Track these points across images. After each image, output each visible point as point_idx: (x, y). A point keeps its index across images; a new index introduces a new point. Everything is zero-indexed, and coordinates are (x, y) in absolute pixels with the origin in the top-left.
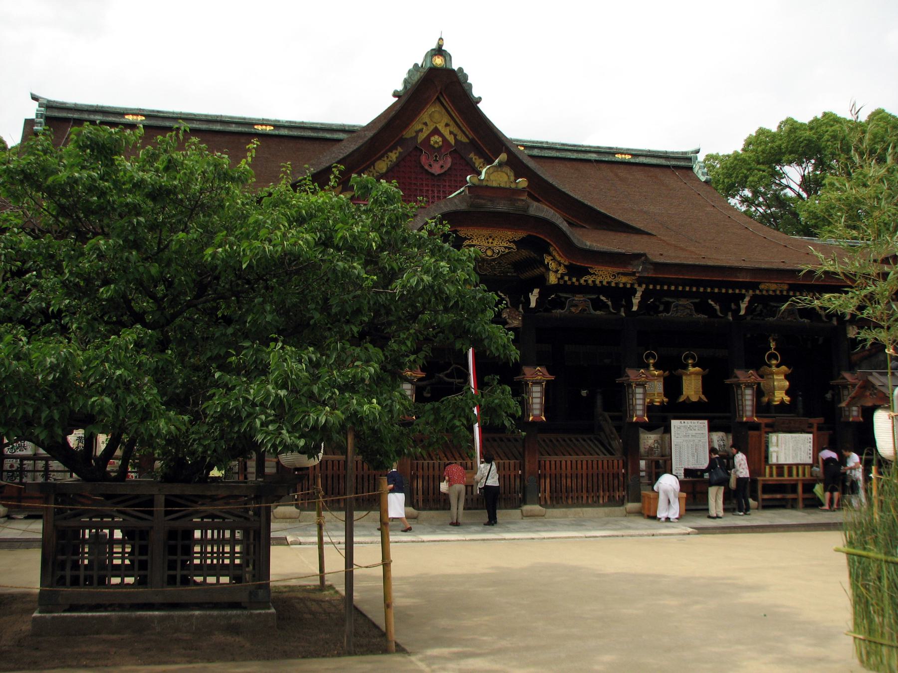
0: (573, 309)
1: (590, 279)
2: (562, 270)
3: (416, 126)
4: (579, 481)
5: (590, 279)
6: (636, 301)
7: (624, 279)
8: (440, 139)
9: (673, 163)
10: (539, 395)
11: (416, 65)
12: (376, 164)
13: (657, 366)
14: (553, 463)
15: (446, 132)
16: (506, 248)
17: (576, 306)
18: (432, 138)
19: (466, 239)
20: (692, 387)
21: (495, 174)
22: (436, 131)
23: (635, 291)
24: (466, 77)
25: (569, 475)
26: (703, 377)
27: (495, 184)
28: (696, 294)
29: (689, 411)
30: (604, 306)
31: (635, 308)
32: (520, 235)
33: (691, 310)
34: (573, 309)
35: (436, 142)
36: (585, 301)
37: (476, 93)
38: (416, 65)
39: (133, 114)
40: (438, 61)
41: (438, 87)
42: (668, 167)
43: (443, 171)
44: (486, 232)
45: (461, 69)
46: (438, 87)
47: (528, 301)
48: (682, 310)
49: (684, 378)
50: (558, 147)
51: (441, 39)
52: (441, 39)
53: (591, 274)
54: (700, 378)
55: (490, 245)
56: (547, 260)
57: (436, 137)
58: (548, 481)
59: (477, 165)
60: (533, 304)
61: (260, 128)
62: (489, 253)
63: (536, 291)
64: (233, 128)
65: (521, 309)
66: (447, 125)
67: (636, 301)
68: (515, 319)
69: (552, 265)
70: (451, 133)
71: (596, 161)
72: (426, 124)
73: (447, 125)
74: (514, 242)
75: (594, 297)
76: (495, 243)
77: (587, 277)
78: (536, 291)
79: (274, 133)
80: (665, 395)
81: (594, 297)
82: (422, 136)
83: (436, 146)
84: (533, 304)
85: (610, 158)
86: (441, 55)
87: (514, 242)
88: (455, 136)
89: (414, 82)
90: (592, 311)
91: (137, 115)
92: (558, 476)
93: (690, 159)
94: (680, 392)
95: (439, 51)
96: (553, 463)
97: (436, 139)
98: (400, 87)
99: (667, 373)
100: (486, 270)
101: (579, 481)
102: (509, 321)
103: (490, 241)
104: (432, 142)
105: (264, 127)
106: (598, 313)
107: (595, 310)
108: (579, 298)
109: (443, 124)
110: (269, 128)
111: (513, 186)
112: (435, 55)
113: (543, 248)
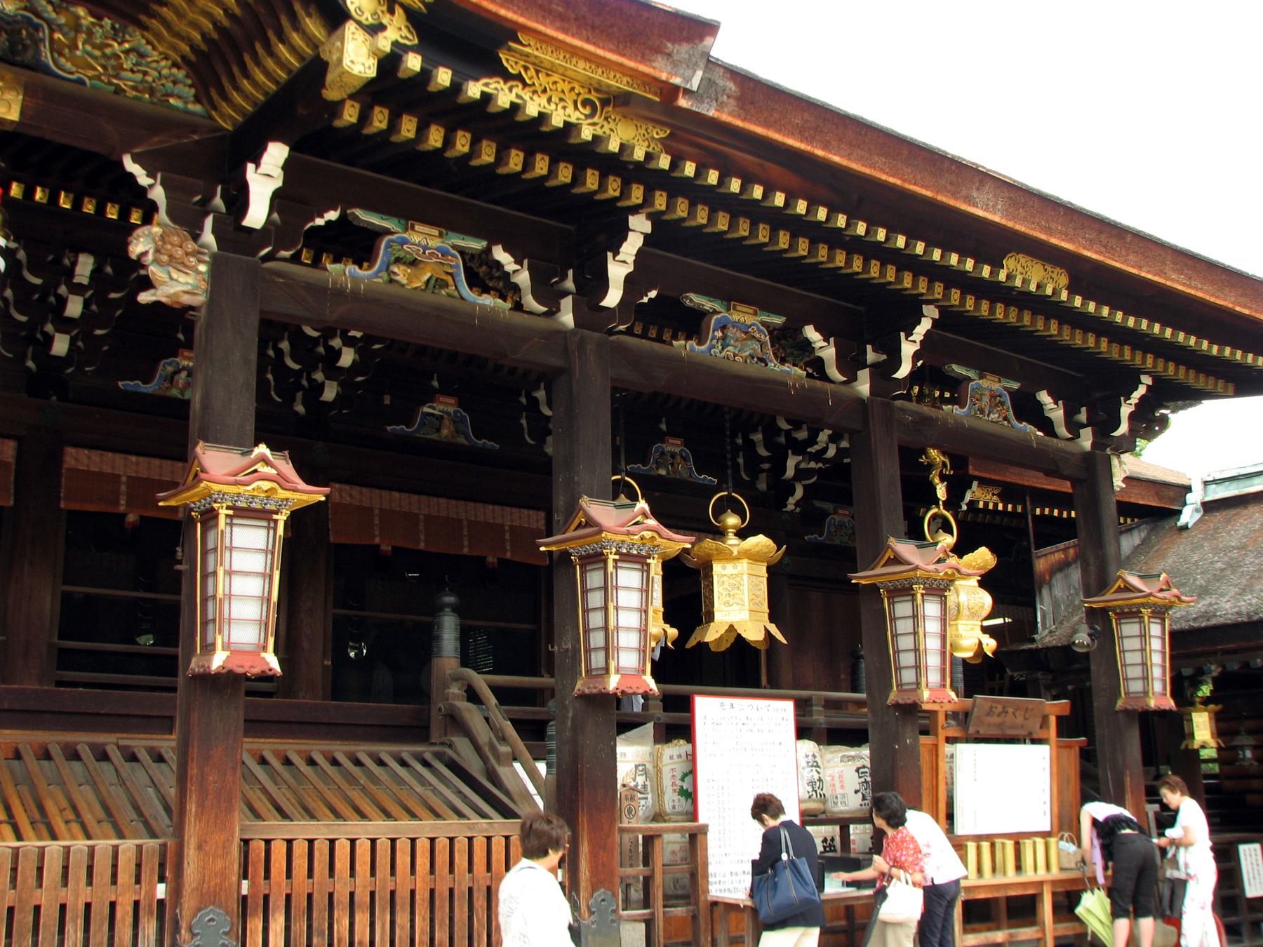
4: (402, 919)
6: (618, 270)
10: (257, 563)
14: (300, 849)
20: (740, 601)
23: (622, 233)
25: (362, 898)
26: (769, 569)
29: (740, 669)
30: (507, 288)
31: (613, 298)
33: (762, 345)
49: (717, 568)
53: (507, 76)
54: (762, 570)
58: (277, 924)
63: (276, 154)
65: (208, 237)
67: (618, 270)
68: (181, 266)
75: (477, 245)
78: (276, 154)
81: (477, 245)
92: (320, 903)
96: (300, 849)
101: (402, 919)
102: (155, 271)
106: (488, 300)
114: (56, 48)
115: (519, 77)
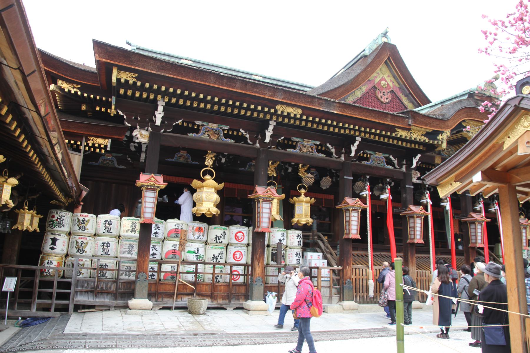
3: (375, 74)
15: (388, 80)
18: (382, 82)
22: (383, 79)
41: (387, 55)
70: (391, 81)
82: (377, 80)
83: (384, 87)
104: (382, 84)
109: (387, 76)
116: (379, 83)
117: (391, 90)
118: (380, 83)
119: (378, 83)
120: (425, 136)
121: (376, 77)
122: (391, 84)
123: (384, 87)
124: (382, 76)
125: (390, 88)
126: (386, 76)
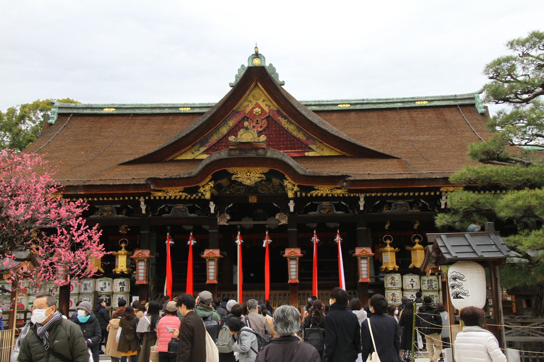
0: (322, 211)
1: (314, 193)
2: (296, 189)
5: (314, 193)
7: (339, 191)
8: (260, 110)
9: (460, 102)
11: (243, 66)
12: (220, 130)
13: (391, 245)
16: (259, 177)
17: (324, 209)
18: (255, 110)
19: (233, 174)
21: (245, 134)
24: (274, 69)
27: (245, 141)
28: (409, 197)
31: (362, 208)
32: (266, 170)
33: (407, 207)
34: (322, 211)
35: (257, 113)
36: (330, 206)
37: (281, 79)
38: (243, 66)
39: (108, 108)
40: (257, 62)
41: (257, 77)
42: (455, 106)
43: (262, 129)
44: (245, 169)
45: (271, 65)
46: (257, 77)
47: (289, 208)
48: (399, 208)
50: (374, 102)
51: (256, 48)
52: (256, 48)
53: (315, 190)
55: (249, 177)
56: (286, 183)
57: (257, 109)
59: (283, 124)
60: (292, 210)
61: (182, 109)
62: (249, 182)
64: (167, 111)
66: (264, 101)
69: (290, 186)
70: (266, 105)
71: (400, 108)
72: (250, 101)
73: (264, 101)
74: (264, 174)
76: (252, 175)
77: (313, 192)
79: (190, 112)
80: (397, 264)
81: (337, 202)
82: (248, 110)
83: (257, 114)
84: (292, 210)
85: (412, 105)
86: (258, 58)
87: (264, 174)
88: (269, 106)
89: (241, 76)
90: (335, 212)
91: (111, 108)
93: (473, 98)
94: (381, 264)
95: (257, 55)
97: (257, 110)
98: (233, 81)
99: (397, 249)
100: (264, 191)
103: (249, 174)
105: (185, 109)
106: (339, 212)
107: (337, 211)
108: (325, 203)
110: (188, 109)
111: (256, 141)
112: (255, 58)
113: (282, 178)
114: (261, 189)
115: (318, 189)
116: (251, 111)
117: (267, 115)
118: (253, 112)
119: (249, 112)
120: (183, 192)
121: (248, 106)
122: (266, 109)
123: (257, 114)
124: (255, 103)
125: (266, 113)
126: (260, 102)
